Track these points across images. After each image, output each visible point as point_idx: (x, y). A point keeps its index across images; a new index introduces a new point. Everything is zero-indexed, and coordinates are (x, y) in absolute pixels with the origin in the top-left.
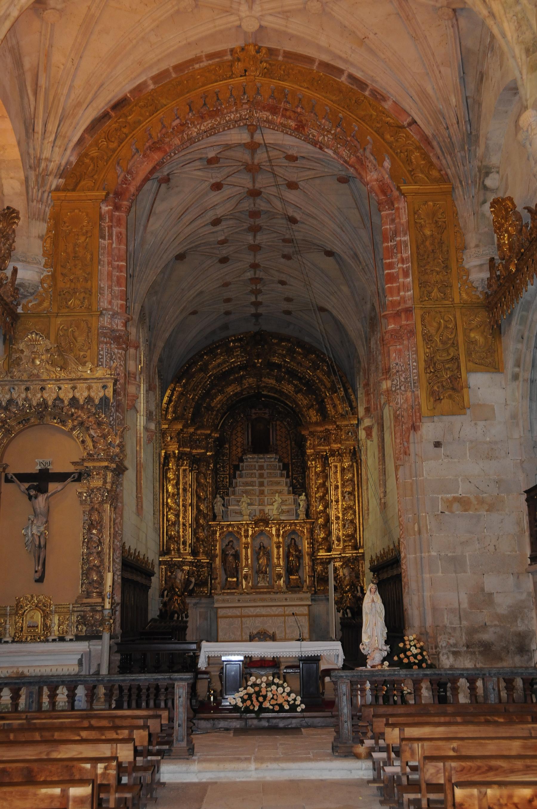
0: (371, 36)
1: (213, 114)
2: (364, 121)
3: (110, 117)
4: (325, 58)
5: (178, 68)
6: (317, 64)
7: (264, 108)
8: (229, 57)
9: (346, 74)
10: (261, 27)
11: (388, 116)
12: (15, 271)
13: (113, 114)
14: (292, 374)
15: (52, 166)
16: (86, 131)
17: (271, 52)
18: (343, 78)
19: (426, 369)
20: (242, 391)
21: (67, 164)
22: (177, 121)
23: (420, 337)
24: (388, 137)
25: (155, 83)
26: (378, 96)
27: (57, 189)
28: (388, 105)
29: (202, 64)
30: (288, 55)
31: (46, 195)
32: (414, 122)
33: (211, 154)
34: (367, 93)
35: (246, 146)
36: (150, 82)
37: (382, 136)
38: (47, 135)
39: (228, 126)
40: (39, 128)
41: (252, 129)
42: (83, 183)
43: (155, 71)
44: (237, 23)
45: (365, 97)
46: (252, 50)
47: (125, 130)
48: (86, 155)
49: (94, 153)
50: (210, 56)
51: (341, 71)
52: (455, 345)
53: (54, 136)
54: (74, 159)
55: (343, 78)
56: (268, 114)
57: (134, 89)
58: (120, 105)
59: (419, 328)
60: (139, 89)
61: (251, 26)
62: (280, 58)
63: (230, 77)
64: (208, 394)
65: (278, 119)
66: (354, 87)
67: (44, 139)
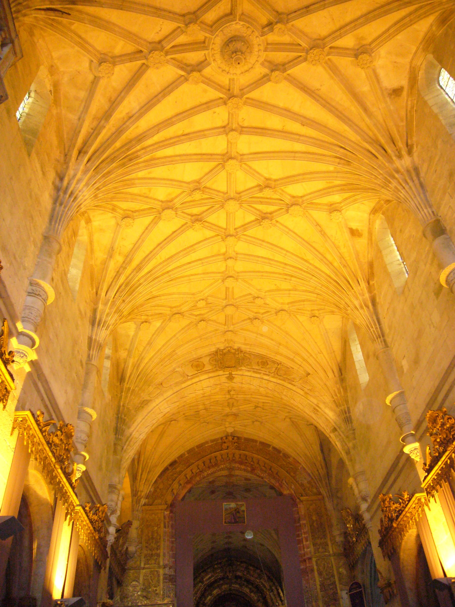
0: (282, 433)
1: (213, 466)
2: (281, 468)
4: (262, 440)
5: (198, 447)
6: (258, 443)
7: (236, 462)
8: (220, 441)
9: (271, 447)
10: (234, 430)
11: (291, 465)
12: (127, 548)
13: (170, 468)
14: (248, 581)
15: (143, 494)
16: (159, 477)
17: (238, 438)
18: (270, 449)
19: (321, 589)
20: (222, 592)
21: (150, 491)
22: (198, 470)
23: (316, 573)
24: (292, 474)
25: (188, 453)
26: (286, 456)
27: (145, 505)
31: (140, 507)
33: (211, 480)
34: (281, 455)
37: (289, 474)
38: (142, 480)
40: (139, 478)
42: (156, 501)
44: (225, 429)
45: (281, 456)
46: (230, 438)
47: (175, 475)
48: (158, 487)
49: (161, 486)
50: (212, 441)
51: (269, 446)
52: (333, 576)
53: (144, 481)
54: (152, 490)
55: (270, 449)
58: (173, 464)
59: (315, 567)
60: (181, 456)
62: (243, 441)
63: (221, 450)
64: (203, 595)
65: (243, 467)
67: (140, 482)
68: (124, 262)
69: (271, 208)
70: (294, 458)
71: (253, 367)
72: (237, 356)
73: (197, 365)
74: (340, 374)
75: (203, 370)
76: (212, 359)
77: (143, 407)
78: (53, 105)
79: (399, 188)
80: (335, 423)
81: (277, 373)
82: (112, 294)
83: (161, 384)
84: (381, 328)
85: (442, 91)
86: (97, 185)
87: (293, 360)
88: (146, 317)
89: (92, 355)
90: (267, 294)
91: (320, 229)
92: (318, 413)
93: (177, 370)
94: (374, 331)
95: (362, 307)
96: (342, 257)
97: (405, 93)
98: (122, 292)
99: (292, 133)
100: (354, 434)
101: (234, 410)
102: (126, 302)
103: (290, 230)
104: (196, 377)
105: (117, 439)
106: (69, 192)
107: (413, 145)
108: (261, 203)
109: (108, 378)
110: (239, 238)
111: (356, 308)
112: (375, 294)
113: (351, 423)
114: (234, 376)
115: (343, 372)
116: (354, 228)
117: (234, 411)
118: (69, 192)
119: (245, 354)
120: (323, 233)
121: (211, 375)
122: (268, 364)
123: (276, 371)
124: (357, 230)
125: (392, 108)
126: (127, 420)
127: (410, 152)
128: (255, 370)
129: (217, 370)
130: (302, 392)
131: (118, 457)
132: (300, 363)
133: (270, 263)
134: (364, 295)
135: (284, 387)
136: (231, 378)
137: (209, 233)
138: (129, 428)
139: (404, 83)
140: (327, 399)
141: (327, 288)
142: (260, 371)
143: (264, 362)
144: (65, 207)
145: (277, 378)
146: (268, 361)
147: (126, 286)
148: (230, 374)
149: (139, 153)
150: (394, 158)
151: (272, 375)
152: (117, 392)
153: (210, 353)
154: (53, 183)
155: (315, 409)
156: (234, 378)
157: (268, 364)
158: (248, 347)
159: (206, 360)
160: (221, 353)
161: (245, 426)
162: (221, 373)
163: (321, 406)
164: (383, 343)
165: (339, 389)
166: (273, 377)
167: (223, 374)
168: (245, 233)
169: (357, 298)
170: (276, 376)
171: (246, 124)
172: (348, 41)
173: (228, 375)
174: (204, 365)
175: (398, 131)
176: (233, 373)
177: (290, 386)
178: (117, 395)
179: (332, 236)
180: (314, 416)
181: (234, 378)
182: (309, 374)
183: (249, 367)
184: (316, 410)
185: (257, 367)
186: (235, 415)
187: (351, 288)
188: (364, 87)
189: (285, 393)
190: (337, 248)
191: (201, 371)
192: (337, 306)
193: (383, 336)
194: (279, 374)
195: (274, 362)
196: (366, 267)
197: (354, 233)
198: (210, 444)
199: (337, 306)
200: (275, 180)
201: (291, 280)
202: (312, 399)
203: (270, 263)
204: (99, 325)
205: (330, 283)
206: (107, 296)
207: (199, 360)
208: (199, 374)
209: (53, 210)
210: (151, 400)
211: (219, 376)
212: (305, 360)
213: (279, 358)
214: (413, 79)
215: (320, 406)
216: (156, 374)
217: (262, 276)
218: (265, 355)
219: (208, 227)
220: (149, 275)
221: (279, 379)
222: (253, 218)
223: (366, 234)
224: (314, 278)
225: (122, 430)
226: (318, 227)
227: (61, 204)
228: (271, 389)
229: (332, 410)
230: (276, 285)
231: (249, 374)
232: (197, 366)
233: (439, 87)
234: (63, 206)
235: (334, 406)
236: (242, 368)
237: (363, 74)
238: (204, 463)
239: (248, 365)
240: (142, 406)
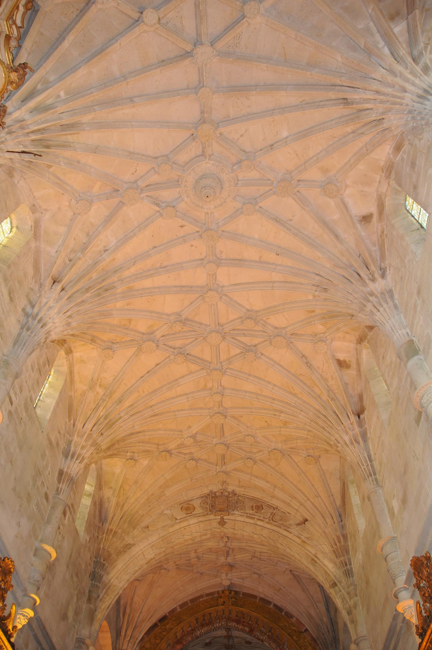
0: (283, 588)
1: (207, 625)
2: (282, 629)
3: (158, 626)
4: (262, 596)
5: (192, 601)
6: (258, 598)
7: (233, 621)
8: (216, 595)
9: (272, 604)
10: (231, 583)
11: (294, 626)
13: (159, 624)
16: (145, 634)
17: (236, 592)
18: (271, 606)
22: (190, 628)
25: (180, 608)
26: (289, 615)
28: (294, 620)
29: (203, 599)
30: (244, 594)
32: (306, 630)
33: (207, 641)
34: (283, 614)
35: (225, 637)
36: (178, 608)
39: (216, 629)
40: (123, 633)
41: (228, 629)
43: (181, 603)
44: (220, 581)
45: (282, 616)
46: (227, 593)
47: (164, 633)
48: (144, 647)
50: (208, 595)
51: (270, 603)
53: (129, 637)
55: (271, 606)
56: (235, 624)
57: (170, 611)
58: (163, 619)
60: (173, 611)
61: (226, 583)
62: (241, 596)
63: (217, 606)
65: (240, 627)
66: (277, 611)
68: (104, 394)
69: (256, 341)
70: (297, 619)
71: (247, 512)
72: (230, 499)
73: (188, 508)
74: (340, 520)
75: (193, 513)
76: (203, 502)
77: (125, 552)
78: (33, 239)
79: (375, 310)
80: (335, 577)
81: (272, 519)
82: (89, 426)
83: (148, 527)
84: (372, 466)
85: (409, 214)
86: (68, 314)
87: (289, 504)
88: (131, 454)
89: (61, 489)
90: (257, 431)
91: (305, 360)
92: (316, 564)
93: (166, 512)
94: (365, 469)
95: (352, 443)
96: (329, 390)
97: (375, 219)
98: (100, 425)
99: (269, 263)
100: (355, 589)
101: (230, 560)
102: (104, 435)
103: (275, 362)
104: (185, 520)
105: (93, 586)
106: (39, 318)
107: (386, 268)
108: (244, 335)
109: (87, 516)
110: (225, 371)
111: (346, 444)
112: (366, 428)
113: (353, 576)
114: (225, 521)
115: (343, 518)
116: (341, 359)
117: (229, 561)
118: (39, 318)
120: (309, 365)
121: (201, 519)
122: (263, 508)
123: (272, 516)
124: (345, 361)
125: (363, 234)
126: (107, 565)
127: (383, 276)
128: (249, 515)
129: (207, 514)
130: (299, 541)
131: (92, 606)
132: (297, 508)
133: (258, 399)
134: (353, 430)
135: (279, 534)
136: (222, 523)
137: (193, 367)
138: (108, 574)
139: (373, 209)
140: (327, 549)
141: (316, 423)
142: (253, 516)
143: (259, 506)
144: (32, 333)
145: (271, 524)
146: (263, 506)
147: (105, 418)
148: (222, 518)
149: (116, 284)
150: (367, 281)
151: (267, 520)
152: (98, 533)
153: (202, 496)
154: (24, 310)
155: (313, 559)
156: (225, 523)
157: (263, 508)
158: (242, 489)
159: (197, 503)
160: (214, 495)
161: (243, 579)
162: (212, 517)
163: (320, 556)
164: (375, 482)
165: (338, 537)
166: (268, 523)
167: (214, 518)
168: (230, 367)
169: (347, 433)
170: (271, 522)
171: (224, 256)
172: (314, 174)
174: (195, 508)
175: (371, 255)
176: (225, 517)
177: (285, 533)
178: (97, 536)
179: (319, 368)
180: (312, 568)
181: (225, 523)
182: (307, 520)
183: (242, 511)
184: (313, 561)
185: (251, 512)
186: (231, 566)
187: (340, 423)
188: (334, 216)
189: (280, 542)
190: (326, 380)
191: (191, 514)
192: (328, 443)
193: (375, 474)
194: (274, 520)
195: (269, 506)
196: (356, 399)
197: (342, 364)
198: (205, 598)
199: (328, 443)
200: (257, 311)
201: (280, 416)
202: (309, 548)
203: (258, 399)
204: (72, 457)
205: (319, 417)
206: (85, 428)
207: (190, 503)
208: (188, 517)
209: (19, 335)
210: (134, 544)
212: (301, 504)
213: (275, 502)
214: (381, 207)
215: (318, 556)
216: (142, 516)
217: (251, 412)
218: (260, 498)
219: (192, 360)
220: (131, 408)
221: (274, 525)
222: (238, 351)
223: (354, 365)
224: (302, 413)
225: (100, 575)
226: (304, 359)
227: (28, 330)
228: (265, 536)
229: (331, 560)
230: (266, 422)
231: (242, 519)
232: (187, 509)
233: (405, 211)
234: (30, 331)
235: (333, 557)
236: (235, 512)
237: (332, 203)
238: (197, 620)
239: (241, 509)
240: (125, 550)
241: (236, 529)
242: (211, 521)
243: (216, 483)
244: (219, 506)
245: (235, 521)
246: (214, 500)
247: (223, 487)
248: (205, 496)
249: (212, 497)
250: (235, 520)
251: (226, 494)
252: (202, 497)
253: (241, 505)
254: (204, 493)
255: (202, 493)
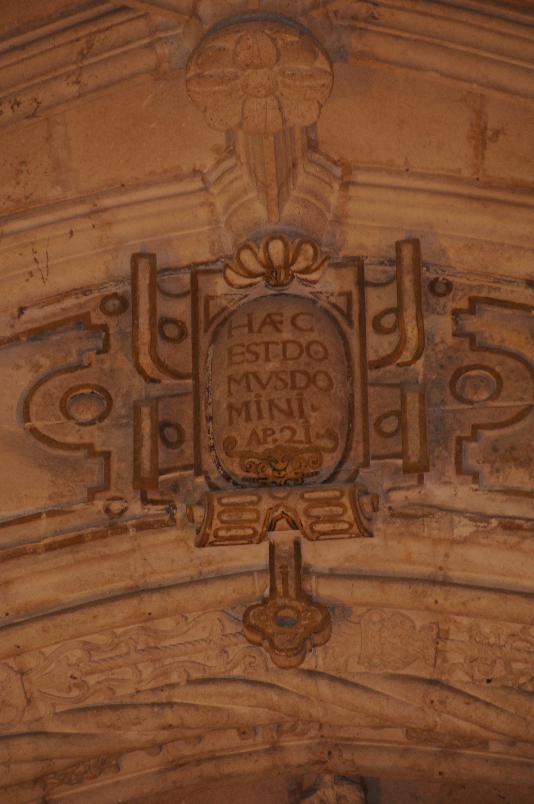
72: (379, 345)
76: (56, 386)
114: (325, 590)
119: (471, 324)
129: (113, 525)
136: (289, 617)
148: (289, 570)
153: (36, 315)
156: (328, 614)
160: (181, 309)
162: (168, 553)
173: (261, 586)
176: (321, 555)
181: (328, 614)
183: (518, 478)
211: (136, 592)
236: (439, 492)
241: (458, 678)
242: (153, 603)
243: (207, 162)
244: (242, 432)
245: (437, 594)
246: (180, 356)
247: (290, 209)
248: (81, 321)
249: (160, 324)
250: (446, 583)
251: (330, 284)
252: (37, 334)
253: (507, 404)
254: (62, 281)
255: (36, 288)
